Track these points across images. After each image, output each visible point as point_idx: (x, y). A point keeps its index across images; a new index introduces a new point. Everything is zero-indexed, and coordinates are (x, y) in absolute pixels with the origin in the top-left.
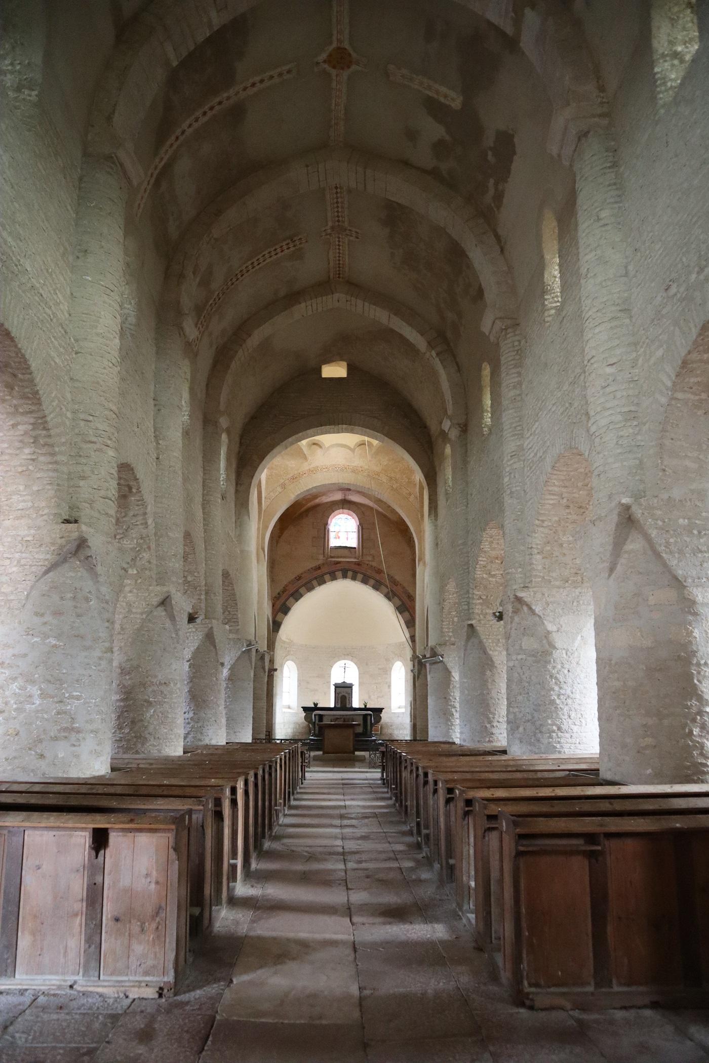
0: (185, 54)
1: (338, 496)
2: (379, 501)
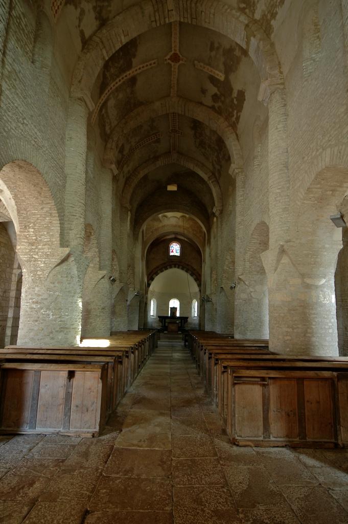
0: (111, 54)
1: (173, 236)
2: (188, 239)
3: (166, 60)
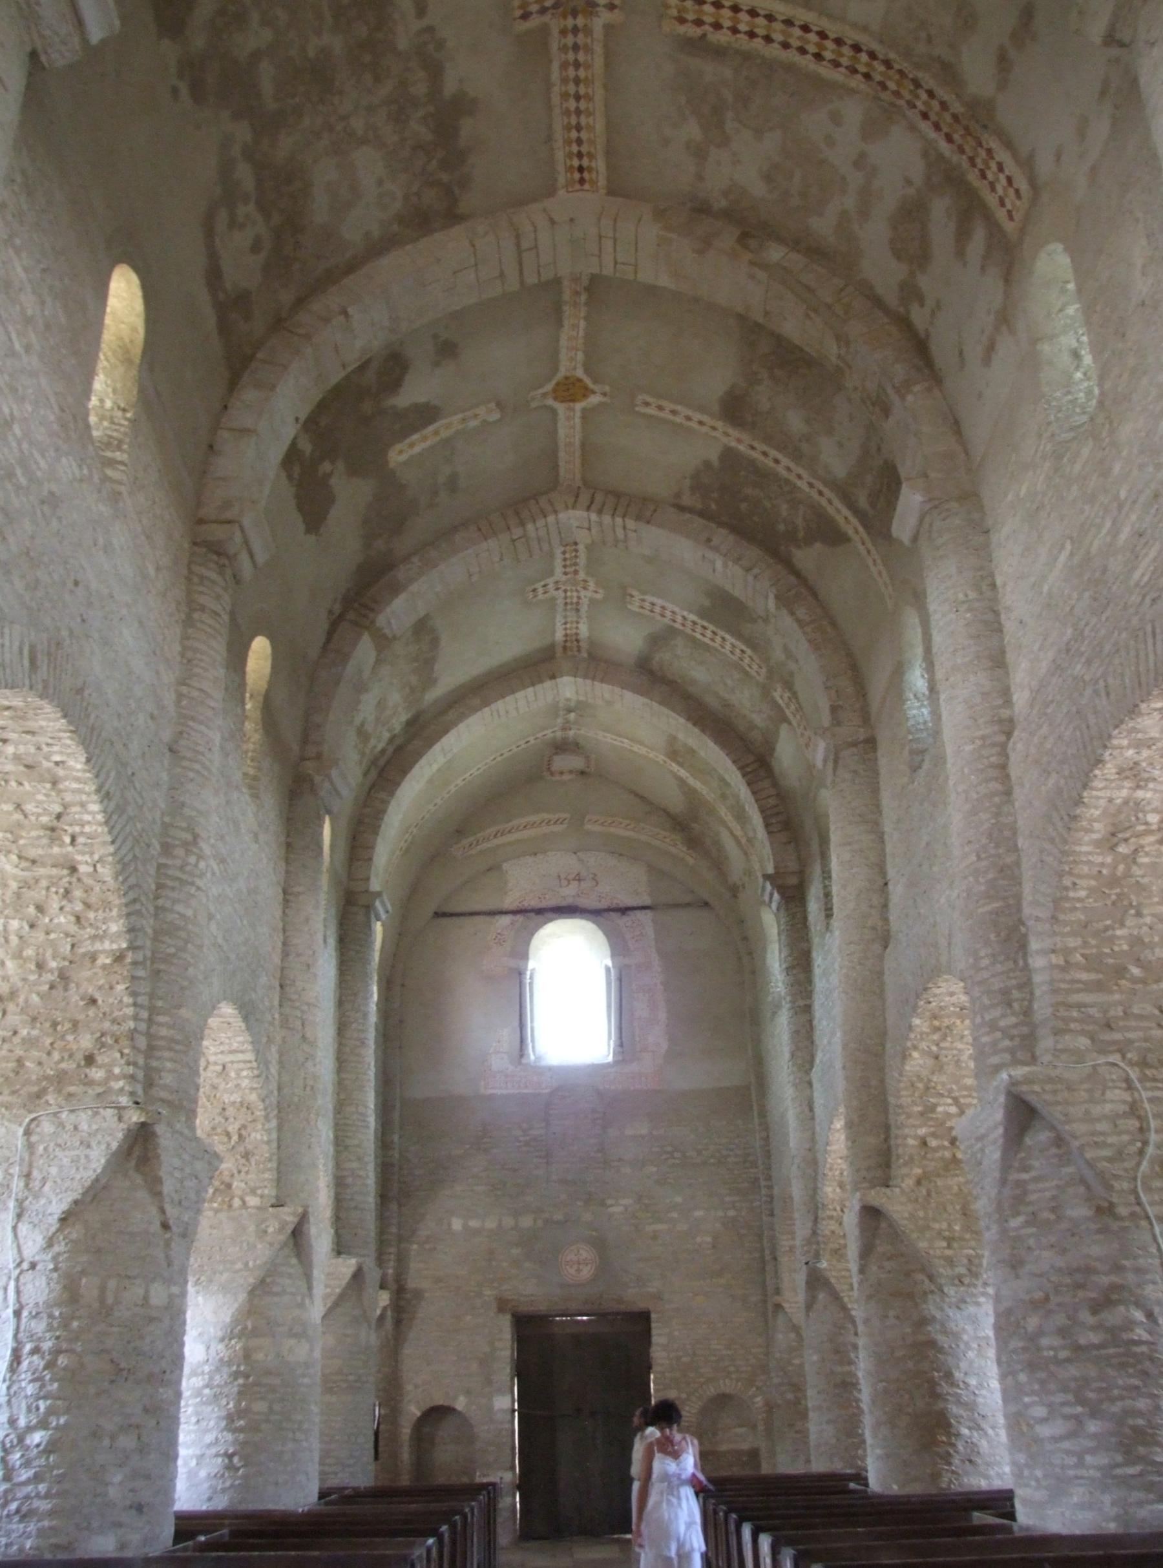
3: (605, 394)
